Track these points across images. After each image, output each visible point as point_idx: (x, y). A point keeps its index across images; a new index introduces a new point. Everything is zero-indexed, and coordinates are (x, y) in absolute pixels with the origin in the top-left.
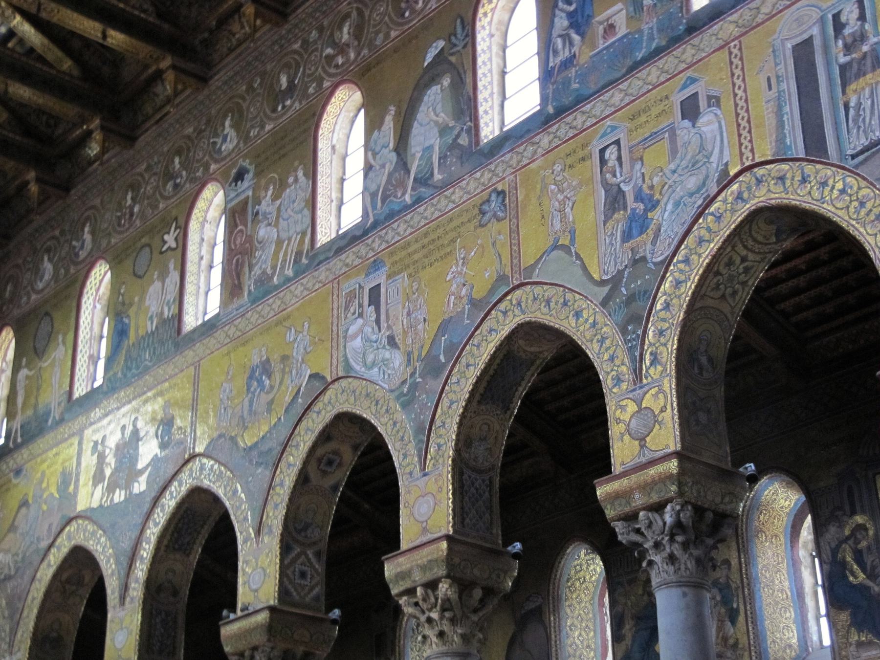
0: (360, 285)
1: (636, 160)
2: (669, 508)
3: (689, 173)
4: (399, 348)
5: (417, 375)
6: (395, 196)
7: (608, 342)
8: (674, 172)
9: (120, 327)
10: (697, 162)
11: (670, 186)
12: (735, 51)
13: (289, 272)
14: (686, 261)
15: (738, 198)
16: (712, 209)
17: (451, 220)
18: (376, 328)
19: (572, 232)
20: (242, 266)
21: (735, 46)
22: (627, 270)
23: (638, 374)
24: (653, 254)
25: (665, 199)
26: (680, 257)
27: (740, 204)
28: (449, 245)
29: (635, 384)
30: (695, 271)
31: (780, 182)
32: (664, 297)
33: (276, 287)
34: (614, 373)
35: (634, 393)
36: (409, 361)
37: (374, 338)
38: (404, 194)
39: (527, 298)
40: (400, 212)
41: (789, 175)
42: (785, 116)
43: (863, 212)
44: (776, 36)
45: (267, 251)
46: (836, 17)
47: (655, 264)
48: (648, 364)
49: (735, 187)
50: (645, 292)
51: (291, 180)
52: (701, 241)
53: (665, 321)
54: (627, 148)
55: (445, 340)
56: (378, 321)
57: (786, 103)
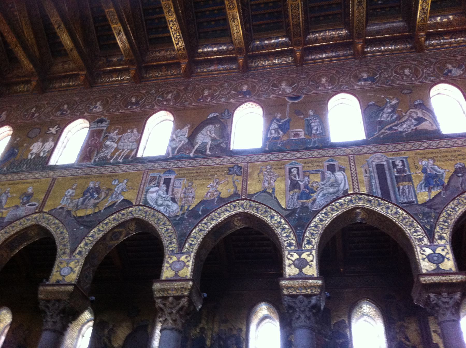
0: (160, 176)
1: (306, 176)
2: (314, 297)
4: (177, 203)
5: (185, 215)
6: (186, 153)
7: (286, 230)
8: (323, 185)
9: (12, 152)
10: (334, 185)
12: (352, 158)
13: (121, 161)
16: (339, 201)
17: (213, 168)
18: (165, 193)
20: (94, 151)
23: (299, 244)
25: (319, 192)
26: (324, 211)
28: (211, 175)
29: (298, 248)
32: (314, 223)
33: (111, 164)
34: (287, 241)
36: (181, 210)
37: (164, 196)
38: (190, 153)
39: (247, 205)
40: (187, 158)
41: (373, 201)
43: (404, 221)
45: (109, 150)
46: (393, 162)
47: (312, 210)
49: (349, 198)
50: (307, 218)
51: (129, 131)
52: (333, 210)
55: (203, 207)
56: (167, 191)
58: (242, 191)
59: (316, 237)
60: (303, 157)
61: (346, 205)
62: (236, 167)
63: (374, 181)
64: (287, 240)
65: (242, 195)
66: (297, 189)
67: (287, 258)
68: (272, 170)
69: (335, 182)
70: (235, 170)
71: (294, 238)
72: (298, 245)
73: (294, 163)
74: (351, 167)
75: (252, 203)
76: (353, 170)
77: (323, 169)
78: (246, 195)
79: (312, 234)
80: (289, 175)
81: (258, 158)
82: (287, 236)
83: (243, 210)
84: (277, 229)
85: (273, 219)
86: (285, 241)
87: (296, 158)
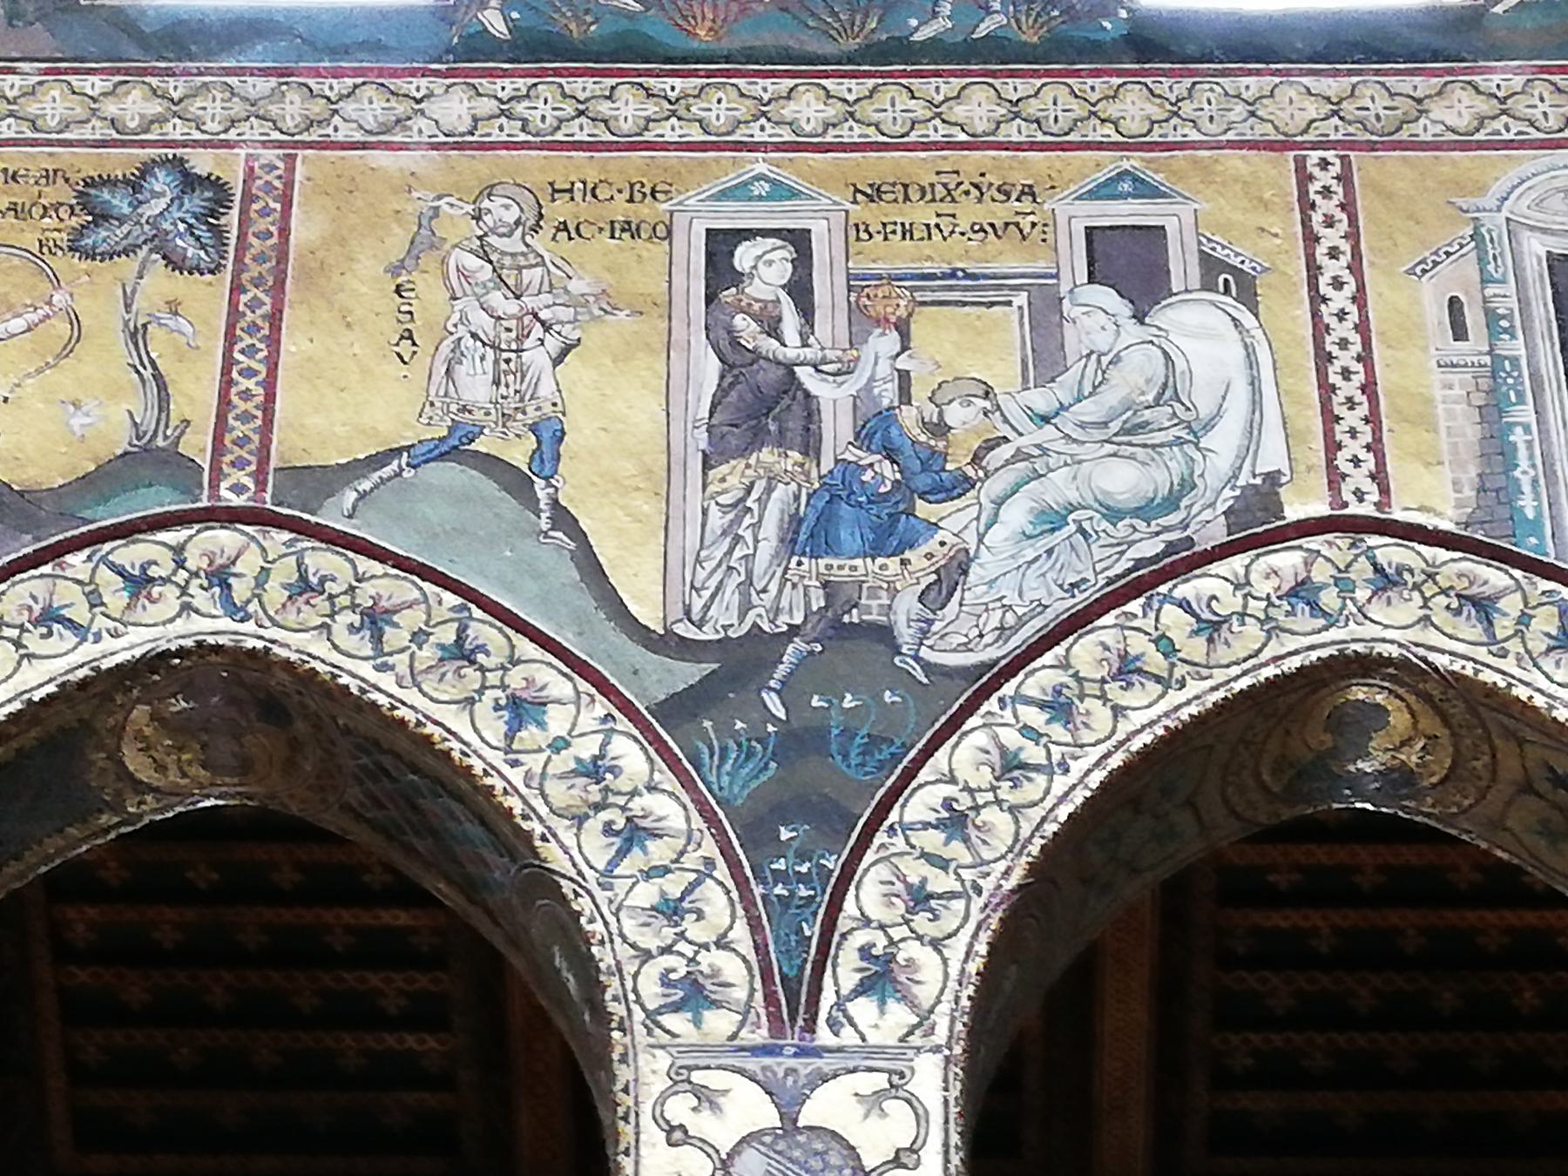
3: (1109, 448)
7: (659, 852)
8: (1046, 419)
11: (1020, 456)
12: (1324, 178)
14: (1059, 707)
15: (1293, 593)
16: (1186, 589)
19: (546, 435)
21: (1324, 164)
22: (798, 644)
24: (925, 634)
26: (1041, 679)
27: (1304, 620)
30: (1095, 753)
31: (1468, 608)
35: (768, 1061)
39: (264, 573)
41: (1511, 605)
42: (1519, 430)
44: (1490, 201)
47: (927, 667)
48: (849, 981)
49: (1287, 561)
52: (1127, 669)
53: (945, 869)
54: (841, 280)
57: (1521, 399)
58: (221, 427)
59: (949, 922)
60: (852, 133)
61: (1252, 627)
62: (162, 182)
63: (1527, 413)
64: (667, 950)
65: (217, 474)
66: (781, 442)
67: (659, 1119)
68: (539, 243)
69: (1157, 403)
70: (155, 207)
71: (741, 934)
72: (770, 998)
73: (762, 188)
74: (1314, 270)
75: (324, 561)
76: (1340, 300)
77: (1041, 266)
78: (260, 478)
79: (920, 898)
80: (710, 299)
81: (402, 108)
82: (671, 910)
83: (226, 623)
84: (568, 838)
85: (529, 735)
86: (646, 956)
87: (788, 136)
